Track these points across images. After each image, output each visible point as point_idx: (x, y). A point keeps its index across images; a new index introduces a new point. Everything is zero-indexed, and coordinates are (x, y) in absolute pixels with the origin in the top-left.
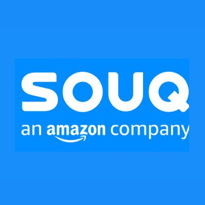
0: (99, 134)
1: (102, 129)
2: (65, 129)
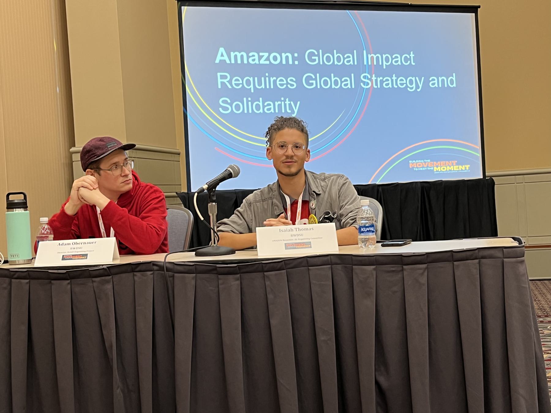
0: (284, 62)
1: (287, 58)
2: (242, 57)
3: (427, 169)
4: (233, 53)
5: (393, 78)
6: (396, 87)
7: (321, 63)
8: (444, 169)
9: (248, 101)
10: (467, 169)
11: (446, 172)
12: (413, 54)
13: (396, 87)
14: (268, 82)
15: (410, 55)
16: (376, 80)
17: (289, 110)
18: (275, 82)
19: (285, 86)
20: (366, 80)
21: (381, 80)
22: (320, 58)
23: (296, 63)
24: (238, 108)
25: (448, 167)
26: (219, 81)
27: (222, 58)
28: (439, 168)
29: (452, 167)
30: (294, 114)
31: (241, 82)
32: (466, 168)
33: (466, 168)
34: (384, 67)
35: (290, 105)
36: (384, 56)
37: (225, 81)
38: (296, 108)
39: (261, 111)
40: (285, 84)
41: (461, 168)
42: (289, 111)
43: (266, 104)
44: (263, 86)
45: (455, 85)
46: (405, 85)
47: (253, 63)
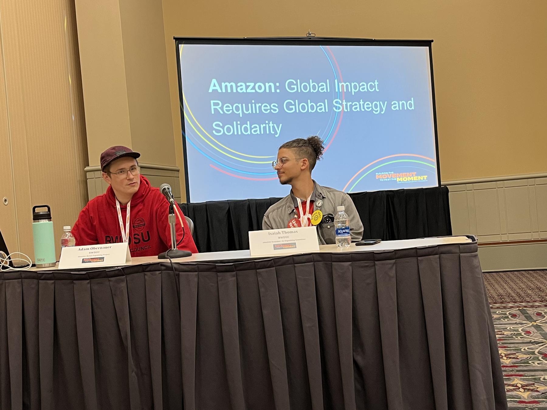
0: (268, 91)
1: (270, 87)
2: (231, 86)
3: (391, 179)
4: (224, 83)
5: (360, 103)
6: (363, 110)
7: (299, 91)
8: (405, 179)
9: (237, 125)
10: (425, 179)
11: (407, 182)
12: (377, 82)
13: (363, 110)
14: (254, 108)
15: (375, 83)
16: (346, 105)
17: (273, 131)
18: (260, 107)
19: (269, 111)
20: (338, 105)
21: (350, 105)
22: (298, 87)
23: (278, 91)
24: (229, 130)
25: (409, 178)
26: (213, 107)
27: (215, 88)
28: (401, 178)
29: (412, 178)
30: (277, 135)
31: (231, 108)
32: (424, 178)
33: (424, 178)
34: (353, 94)
35: (273, 127)
36: (353, 84)
37: (217, 107)
38: (278, 130)
39: (249, 132)
40: (269, 109)
41: (420, 179)
42: (273, 133)
43: (252, 127)
44: (250, 111)
45: (413, 108)
46: (371, 109)
47: (241, 91)
